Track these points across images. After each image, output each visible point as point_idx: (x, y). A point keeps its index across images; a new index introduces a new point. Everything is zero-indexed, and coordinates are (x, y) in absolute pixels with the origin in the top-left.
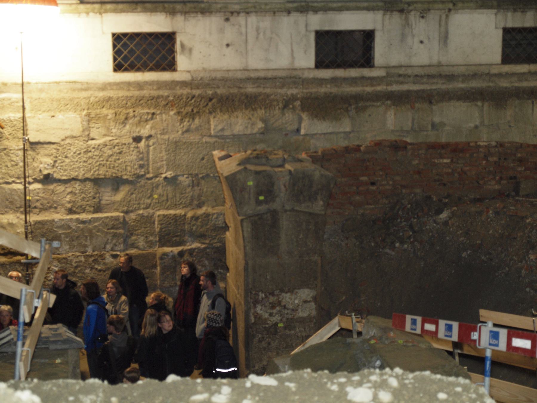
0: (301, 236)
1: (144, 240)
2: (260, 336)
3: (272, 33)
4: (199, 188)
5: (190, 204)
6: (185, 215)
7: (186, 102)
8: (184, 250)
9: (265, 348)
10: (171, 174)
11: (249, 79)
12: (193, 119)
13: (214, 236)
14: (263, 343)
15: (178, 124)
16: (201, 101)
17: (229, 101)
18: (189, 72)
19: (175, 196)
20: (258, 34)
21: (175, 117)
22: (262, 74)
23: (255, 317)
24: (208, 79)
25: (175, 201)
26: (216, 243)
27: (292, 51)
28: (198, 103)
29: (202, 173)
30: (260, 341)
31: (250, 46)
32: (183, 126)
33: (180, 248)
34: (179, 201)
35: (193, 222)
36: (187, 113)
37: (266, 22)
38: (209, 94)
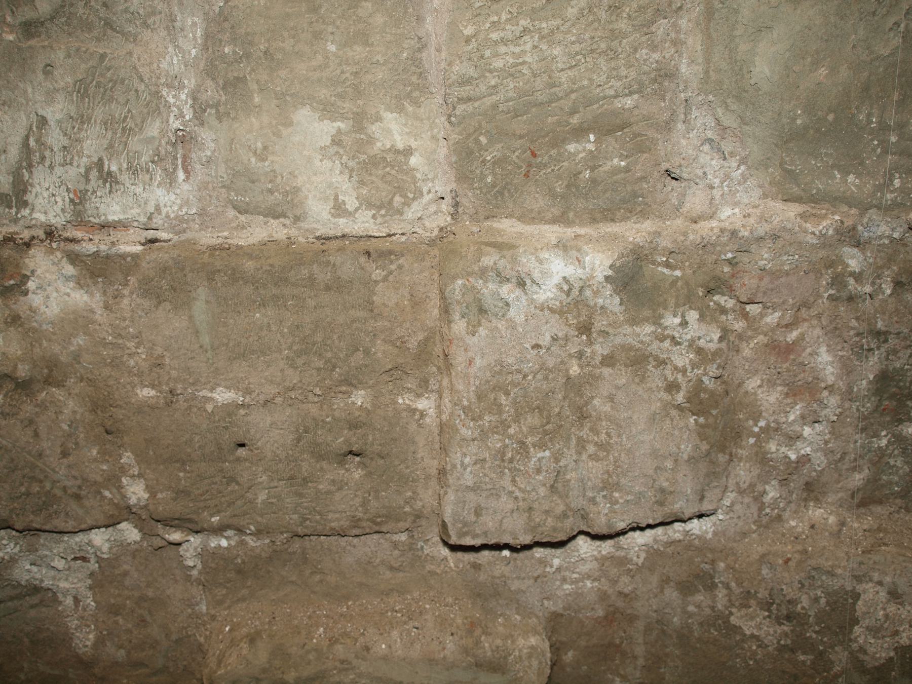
1: (336, 141)
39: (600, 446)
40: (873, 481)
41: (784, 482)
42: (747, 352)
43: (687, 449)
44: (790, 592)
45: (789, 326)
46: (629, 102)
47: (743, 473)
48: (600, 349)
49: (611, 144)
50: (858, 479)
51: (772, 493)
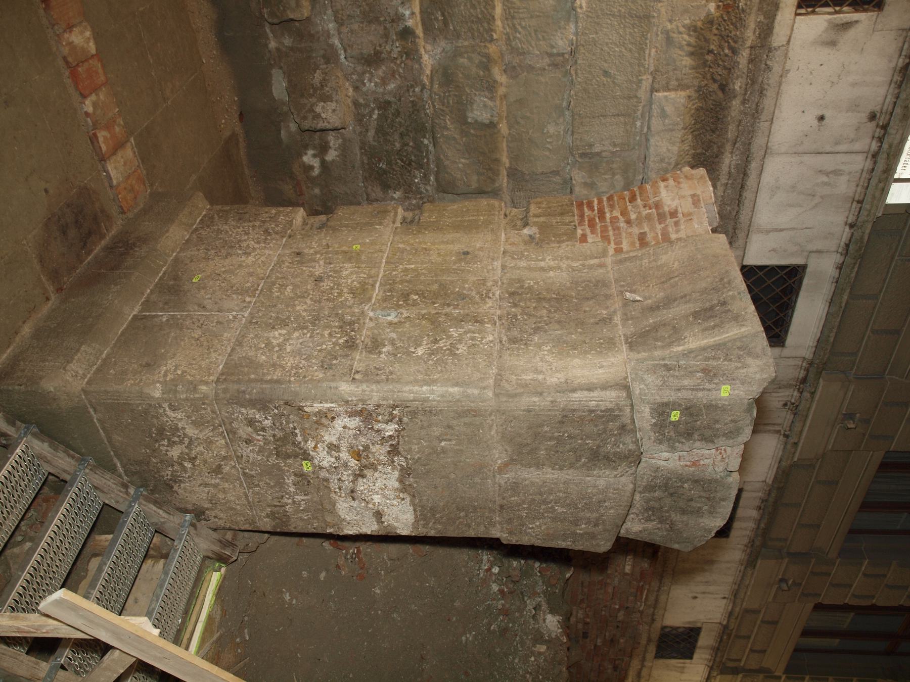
0: (559, 509)
2: (268, 423)
3: (822, 197)
4: (547, 67)
5: (513, 48)
6: (492, 40)
7: (728, 36)
8: (417, 40)
9: (232, 432)
10: (581, 7)
11: (747, 159)
12: (692, 54)
13: (448, 103)
14: (250, 429)
15: (687, 22)
16: (725, 68)
17: (713, 123)
18: (789, 41)
19: (532, 17)
20: (827, 174)
21: (703, 15)
22: (751, 181)
23: (322, 414)
24: (765, 81)
25: (521, 15)
26: (434, 106)
27: (782, 230)
28: (721, 63)
29: (576, 74)
30: (251, 422)
31: (806, 158)
32: (680, 33)
33: (419, 31)
34: (520, 24)
35: (477, 59)
36: (707, 41)
37: (844, 187)
38: (734, 84)
39: (362, 27)
40: (361, 105)
41: (357, 80)
42: (392, 65)
43: (365, 51)
44: (329, 85)
45: (400, 76)
46: (451, 28)
47: (359, 68)
48: (388, 26)
49: (441, 24)
50: (361, 101)
51: (354, 77)
